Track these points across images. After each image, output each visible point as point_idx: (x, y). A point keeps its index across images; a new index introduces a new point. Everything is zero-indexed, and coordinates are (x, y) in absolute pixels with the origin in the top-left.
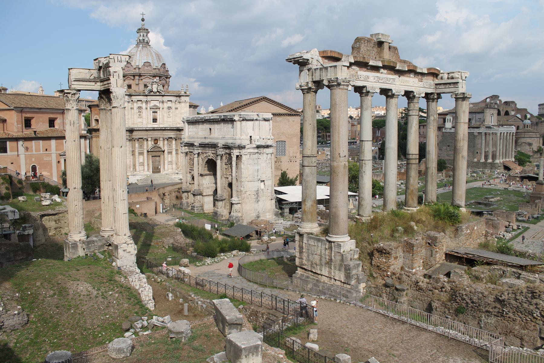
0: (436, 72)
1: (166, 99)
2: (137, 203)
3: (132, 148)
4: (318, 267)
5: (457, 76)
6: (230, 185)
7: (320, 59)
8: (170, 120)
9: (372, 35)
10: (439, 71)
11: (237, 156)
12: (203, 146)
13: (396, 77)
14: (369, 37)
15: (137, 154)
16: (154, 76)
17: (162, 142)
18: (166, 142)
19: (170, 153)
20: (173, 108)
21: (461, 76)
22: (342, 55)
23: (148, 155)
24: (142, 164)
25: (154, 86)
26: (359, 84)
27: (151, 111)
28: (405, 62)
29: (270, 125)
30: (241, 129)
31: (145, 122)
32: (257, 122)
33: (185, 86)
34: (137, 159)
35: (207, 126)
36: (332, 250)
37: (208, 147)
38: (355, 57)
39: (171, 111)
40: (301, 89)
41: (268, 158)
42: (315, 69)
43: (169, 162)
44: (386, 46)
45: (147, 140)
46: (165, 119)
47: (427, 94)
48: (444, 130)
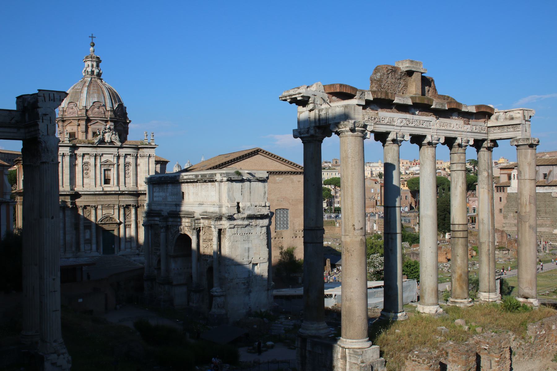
0: (488, 111)
1: (123, 152)
5: (518, 115)
7: (326, 95)
10: (492, 109)
13: (432, 118)
17: (116, 211)
21: (524, 116)
22: (356, 90)
25: (106, 135)
26: (381, 129)
28: (443, 97)
29: (265, 187)
36: (346, 361)
38: (373, 92)
40: (301, 138)
41: (263, 232)
45: (96, 209)
47: (475, 141)
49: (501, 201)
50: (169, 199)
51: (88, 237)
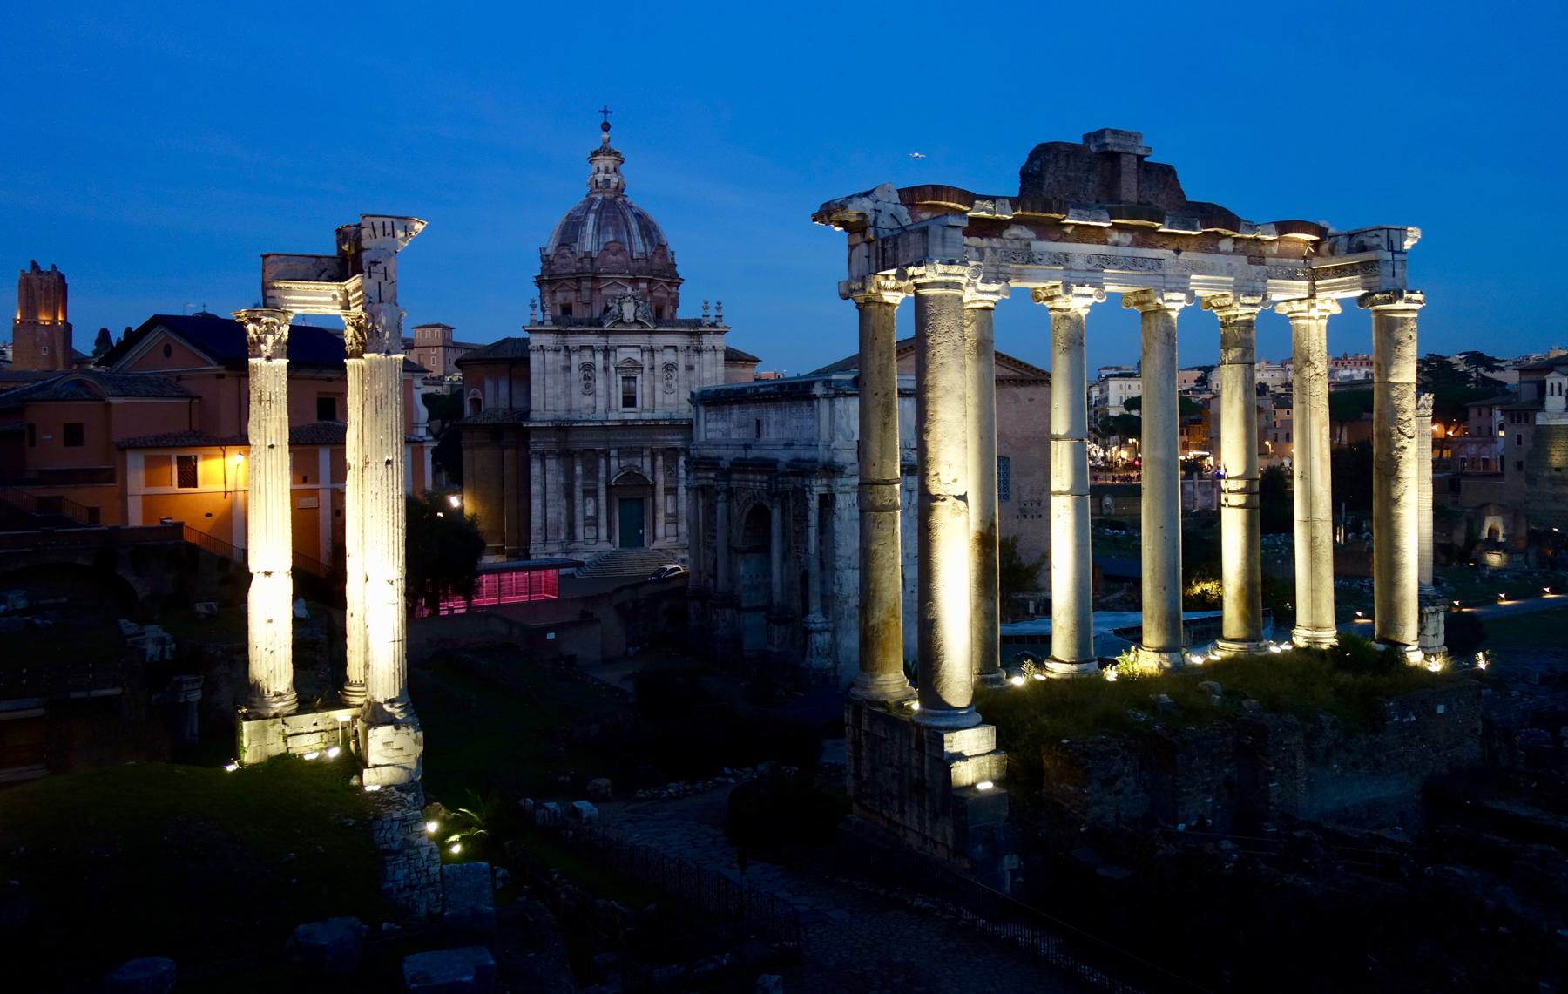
1: (659, 341)
2: (550, 629)
3: (566, 478)
4: (896, 803)
5: (1375, 241)
6: (805, 578)
7: (903, 210)
8: (671, 399)
9: (1087, 137)
11: (822, 497)
12: (740, 466)
14: (1079, 141)
15: (578, 494)
16: (635, 282)
17: (647, 462)
19: (671, 491)
20: (681, 367)
23: (609, 496)
24: (593, 522)
27: (620, 377)
30: (832, 419)
31: (601, 406)
33: (712, 305)
34: (578, 509)
35: (752, 412)
37: (752, 472)
39: (674, 374)
42: (884, 241)
43: (667, 515)
44: (1128, 166)
45: (608, 457)
48: (1540, 419)
49: (1519, 443)
50: (734, 436)
51: (590, 512)
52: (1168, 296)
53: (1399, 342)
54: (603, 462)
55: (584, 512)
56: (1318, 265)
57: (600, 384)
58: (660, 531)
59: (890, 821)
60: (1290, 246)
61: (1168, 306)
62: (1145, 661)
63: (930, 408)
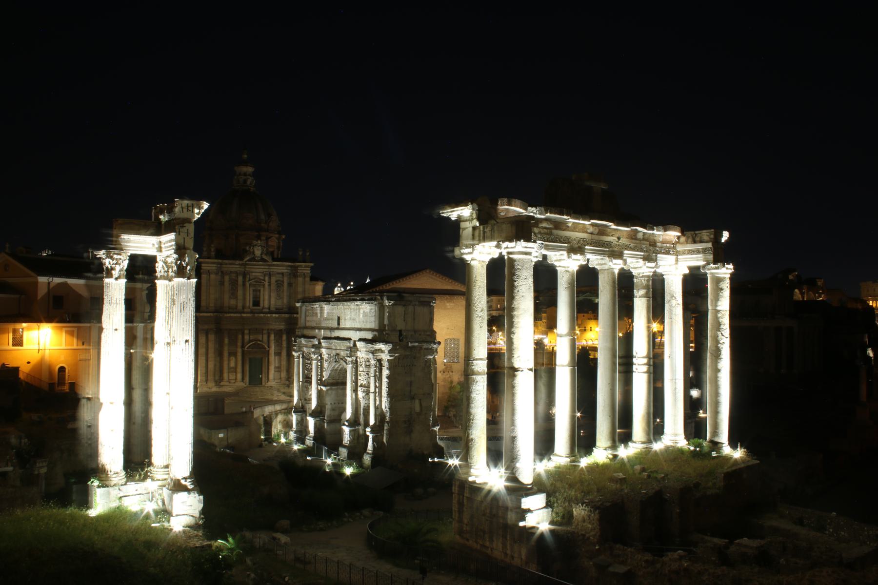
15: (226, 354)
17: (265, 337)
18: (272, 337)
20: (286, 284)
27: (251, 289)
32: (410, 308)
34: (225, 363)
43: (275, 367)
46: (273, 302)
51: (232, 364)
52: (615, 261)
53: (722, 289)
54: (240, 336)
55: (229, 364)
56: (680, 248)
57: (240, 293)
58: (271, 376)
59: (483, 546)
60: (667, 238)
61: (614, 266)
62: (600, 455)
63: (516, 320)
